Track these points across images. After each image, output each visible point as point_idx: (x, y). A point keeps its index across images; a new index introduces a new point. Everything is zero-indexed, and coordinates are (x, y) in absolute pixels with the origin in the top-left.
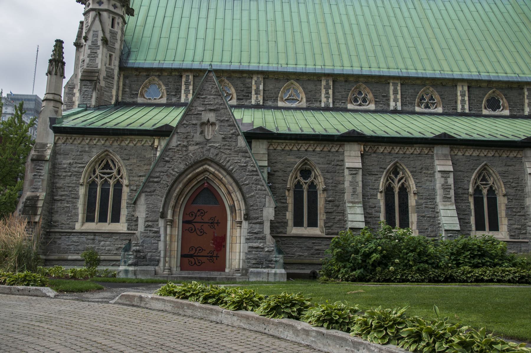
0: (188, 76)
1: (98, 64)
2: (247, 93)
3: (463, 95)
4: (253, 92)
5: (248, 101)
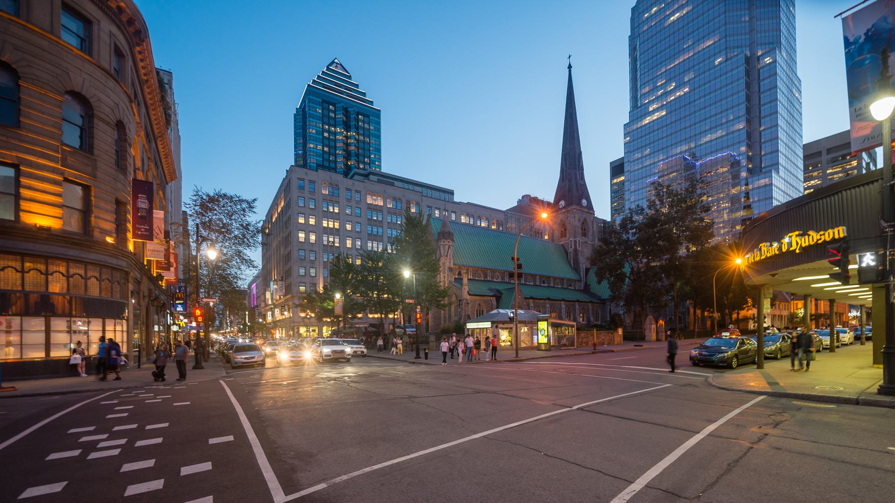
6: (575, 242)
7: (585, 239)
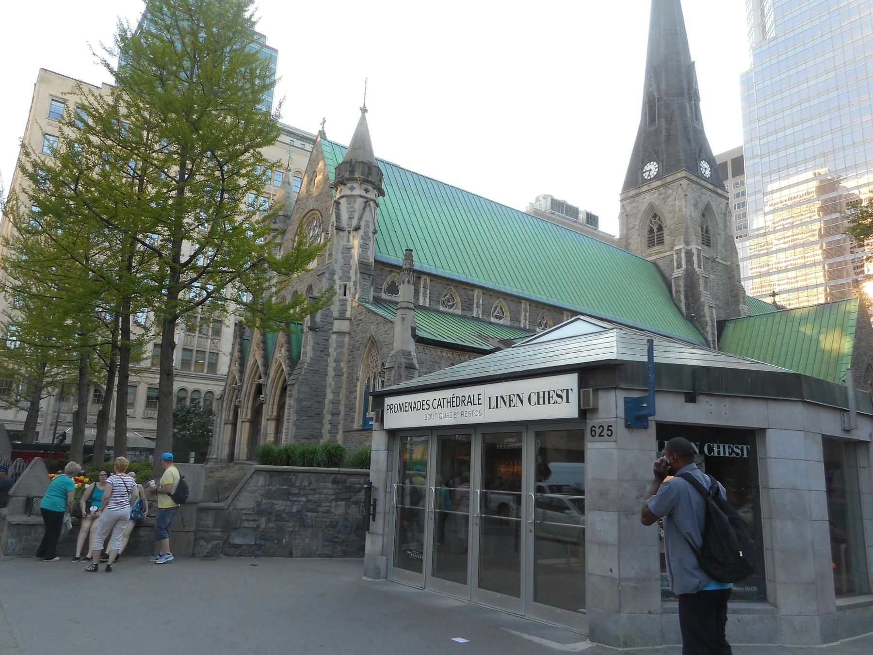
0: (426, 279)
1: (369, 256)
2: (469, 304)
4: (475, 306)
5: (470, 312)
7: (707, 252)
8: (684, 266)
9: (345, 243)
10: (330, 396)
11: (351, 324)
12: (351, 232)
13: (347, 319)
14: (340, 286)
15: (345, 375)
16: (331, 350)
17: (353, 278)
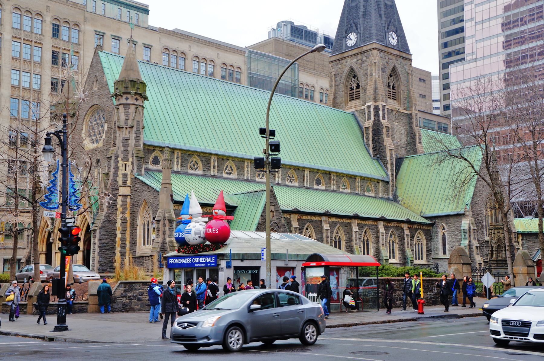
1: (140, 144)
3: (307, 177)
4: (212, 167)
6: (376, 109)
8: (373, 118)
9: (124, 136)
10: (119, 236)
11: (131, 190)
12: (128, 128)
13: (129, 186)
14: (122, 165)
15: (129, 222)
16: (118, 206)
17: (131, 159)
